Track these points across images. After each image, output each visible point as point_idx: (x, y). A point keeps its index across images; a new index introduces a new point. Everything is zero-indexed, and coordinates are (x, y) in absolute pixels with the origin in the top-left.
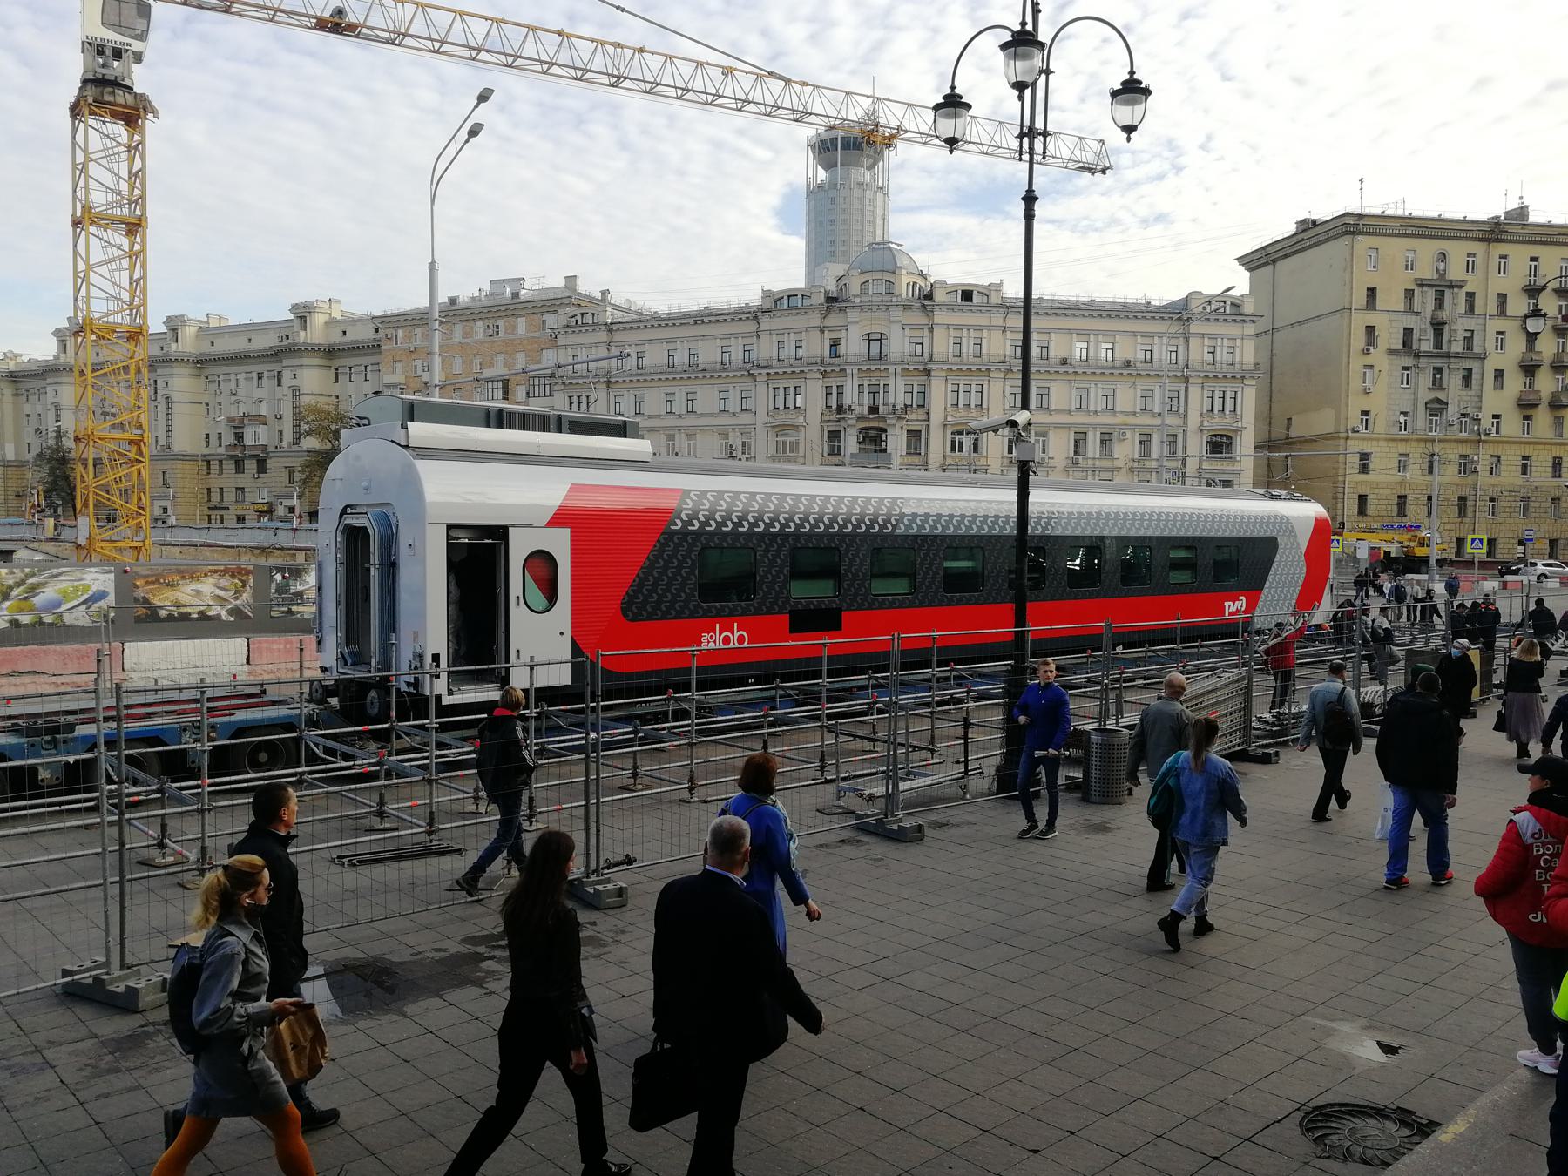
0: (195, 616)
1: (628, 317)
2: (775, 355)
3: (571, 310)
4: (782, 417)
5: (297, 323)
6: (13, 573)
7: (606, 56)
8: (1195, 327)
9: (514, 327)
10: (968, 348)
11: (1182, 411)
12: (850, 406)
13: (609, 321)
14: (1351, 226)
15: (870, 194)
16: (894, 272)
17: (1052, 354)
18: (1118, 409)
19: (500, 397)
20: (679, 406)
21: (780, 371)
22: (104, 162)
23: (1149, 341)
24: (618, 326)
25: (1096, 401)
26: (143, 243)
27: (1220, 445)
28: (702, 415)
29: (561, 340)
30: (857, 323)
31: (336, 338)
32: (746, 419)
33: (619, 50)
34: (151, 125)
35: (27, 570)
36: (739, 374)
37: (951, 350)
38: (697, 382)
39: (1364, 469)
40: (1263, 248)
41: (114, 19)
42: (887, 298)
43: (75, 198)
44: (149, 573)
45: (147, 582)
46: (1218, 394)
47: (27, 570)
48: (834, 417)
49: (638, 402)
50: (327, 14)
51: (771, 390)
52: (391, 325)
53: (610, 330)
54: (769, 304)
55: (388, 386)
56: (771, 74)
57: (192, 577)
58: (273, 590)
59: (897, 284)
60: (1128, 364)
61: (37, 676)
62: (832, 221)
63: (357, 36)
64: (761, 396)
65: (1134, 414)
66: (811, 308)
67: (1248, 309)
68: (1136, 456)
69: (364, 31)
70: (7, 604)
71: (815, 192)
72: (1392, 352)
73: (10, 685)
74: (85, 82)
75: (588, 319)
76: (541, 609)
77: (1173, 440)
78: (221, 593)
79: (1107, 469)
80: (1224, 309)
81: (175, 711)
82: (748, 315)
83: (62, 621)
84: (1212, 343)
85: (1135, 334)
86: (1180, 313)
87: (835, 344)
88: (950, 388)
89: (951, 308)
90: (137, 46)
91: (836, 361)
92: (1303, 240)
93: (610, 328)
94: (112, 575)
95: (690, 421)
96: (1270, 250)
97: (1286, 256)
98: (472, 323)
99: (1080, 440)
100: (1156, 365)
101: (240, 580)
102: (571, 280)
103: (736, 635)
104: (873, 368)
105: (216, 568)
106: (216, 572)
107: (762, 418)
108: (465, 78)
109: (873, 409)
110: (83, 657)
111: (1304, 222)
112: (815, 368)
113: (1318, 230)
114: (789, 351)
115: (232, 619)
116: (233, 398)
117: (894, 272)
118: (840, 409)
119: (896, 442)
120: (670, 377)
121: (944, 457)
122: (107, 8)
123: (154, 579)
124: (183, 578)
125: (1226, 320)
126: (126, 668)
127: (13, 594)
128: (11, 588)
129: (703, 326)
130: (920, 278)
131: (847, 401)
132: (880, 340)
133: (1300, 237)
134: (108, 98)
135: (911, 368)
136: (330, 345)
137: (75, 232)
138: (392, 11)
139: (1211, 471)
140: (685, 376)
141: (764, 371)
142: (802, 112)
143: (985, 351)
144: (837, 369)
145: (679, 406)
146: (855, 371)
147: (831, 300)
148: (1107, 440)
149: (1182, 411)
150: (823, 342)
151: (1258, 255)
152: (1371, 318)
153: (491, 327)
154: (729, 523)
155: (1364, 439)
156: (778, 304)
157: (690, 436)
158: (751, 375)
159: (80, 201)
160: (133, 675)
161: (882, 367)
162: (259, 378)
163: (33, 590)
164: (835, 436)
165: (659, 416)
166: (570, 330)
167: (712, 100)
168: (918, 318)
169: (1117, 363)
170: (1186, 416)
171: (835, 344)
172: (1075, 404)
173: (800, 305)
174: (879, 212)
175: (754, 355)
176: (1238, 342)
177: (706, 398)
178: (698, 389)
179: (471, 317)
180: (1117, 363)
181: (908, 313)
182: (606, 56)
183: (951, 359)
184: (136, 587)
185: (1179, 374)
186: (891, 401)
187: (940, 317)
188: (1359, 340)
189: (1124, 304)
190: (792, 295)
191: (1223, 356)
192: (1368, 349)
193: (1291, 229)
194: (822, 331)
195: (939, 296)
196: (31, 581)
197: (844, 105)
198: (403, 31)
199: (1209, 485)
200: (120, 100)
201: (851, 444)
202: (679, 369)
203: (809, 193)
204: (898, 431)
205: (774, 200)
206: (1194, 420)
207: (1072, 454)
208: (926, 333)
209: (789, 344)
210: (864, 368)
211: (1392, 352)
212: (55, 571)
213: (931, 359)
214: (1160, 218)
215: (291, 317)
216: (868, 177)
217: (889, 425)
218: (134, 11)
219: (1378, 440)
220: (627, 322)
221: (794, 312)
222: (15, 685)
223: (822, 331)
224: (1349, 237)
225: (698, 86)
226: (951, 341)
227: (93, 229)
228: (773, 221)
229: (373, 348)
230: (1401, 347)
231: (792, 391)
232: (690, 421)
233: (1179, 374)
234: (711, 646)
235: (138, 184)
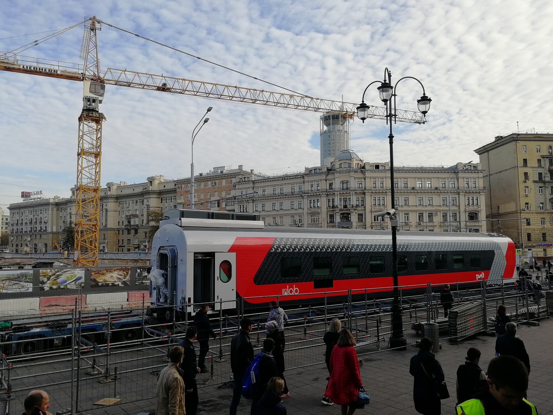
1: (260, 178)
2: (310, 189)
3: (240, 177)
4: (313, 210)
5: (149, 184)
6: (51, 271)
7: (251, 93)
8: (460, 175)
9: (221, 183)
10: (378, 185)
11: (458, 205)
12: (337, 206)
13: (253, 180)
14: (515, 138)
15: (342, 134)
16: (351, 160)
17: (409, 186)
18: (434, 205)
19: (217, 206)
20: (277, 207)
21: (312, 194)
22: (88, 135)
23: (444, 180)
24: (256, 181)
25: (426, 202)
26: (100, 160)
27: (473, 216)
28: (285, 210)
29: (237, 187)
30: (338, 177)
31: (162, 188)
32: (300, 211)
33: (255, 91)
34: (104, 123)
35: (56, 270)
36: (298, 196)
37: (372, 186)
38: (283, 199)
39: (528, 224)
40: (483, 147)
41: (93, 90)
42: (349, 169)
43: (79, 146)
44: (96, 270)
45: (95, 273)
46: (471, 198)
47: (56, 270)
48: (331, 210)
49: (263, 206)
50: (161, 85)
51: (309, 201)
52: (180, 183)
53: (254, 183)
54: (308, 172)
55: (179, 204)
56: (306, 96)
57: (110, 271)
58: (137, 275)
59: (352, 164)
60: (436, 188)
61: (57, 306)
62: (329, 144)
63: (170, 92)
64: (305, 203)
65: (440, 206)
66: (322, 173)
67: (480, 168)
68: (442, 221)
69: (172, 90)
70: (49, 281)
71: (323, 134)
72: (534, 182)
74: (83, 110)
75: (246, 179)
76: (226, 281)
77: (455, 215)
78: (120, 277)
79: (431, 226)
80: (470, 168)
81: (101, 319)
82: (301, 176)
84: (467, 180)
85: (438, 178)
86: (454, 170)
87: (331, 185)
88: (372, 199)
89: (371, 171)
90: (100, 98)
91: (331, 190)
92: (498, 143)
93: (254, 182)
95: (281, 212)
96: (486, 147)
97: (492, 149)
98: (207, 182)
99: (421, 216)
100: (447, 188)
102: (241, 166)
103: (295, 289)
104: (345, 192)
105: (118, 268)
106: (118, 269)
107: (306, 210)
108: (206, 103)
109: (345, 206)
111: (498, 137)
112: (324, 193)
113: (503, 140)
114: (315, 188)
115: (123, 286)
116: (128, 209)
117: (351, 160)
118: (333, 207)
119: (354, 218)
120: (274, 198)
121: (372, 223)
122: (91, 87)
123: (97, 272)
124: (107, 272)
125: (472, 172)
126: (87, 303)
127: (51, 278)
128: (51, 276)
129: (285, 180)
130: (361, 162)
131: (336, 204)
132: (347, 183)
133: (497, 142)
134: (90, 115)
135: (358, 192)
136: (160, 191)
137: (78, 157)
138: (181, 84)
139: (470, 226)
140: (279, 197)
141: (307, 195)
142: (317, 108)
143: (384, 185)
144: (332, 193)
145: (277, 207)
146: (338, 194)
147: (329, 170)
148: (430, 216)
149: (458, 205)
150: (326, 184)
151: (482, 149)
152: (526, 170)
153: (214, 183)
154: (291, 249)
155: (527, 213)
156: (310, 172)
157: (281, 217)
158: (301, 196)
159: (80, 148)
160: (89, 306)
161: (348, 192)
162: (137, 202)
163: (58, 277)
164: (332, 217)
165: (270, 211)
166: (240, 183)
167: (286, 106)
168: (361, 175)
169: (432, 188)
170: (459, 206)
171: (331, 185)
172: (418, 203)
173: (318, 172)
174: (345, 139)
175: (303, 189)
176: (477, 180)
177: (287, 204)
178: (283, 201)
179: (207, 180)
180: (432, 188)
181: (357, 173)
182: (251, 93)
183: (373, 189)
184: (92, 275)
185: (456, 192)
186: (352, 203)
187: (368, 174)
188: (522, 178)
189: (434, 168)
190: (315, 169)
191: (471, 185)
192: (526, 181)
193: (493, 140)
194: (326, 181)
195: (367, 167)
196: (57, 274)
197: (332, 105)
198: (185, 89)
199: (470, 231)
200: (94, 115)
201: (338, 219)
202: (277, 195)
203: (321, 134)
204: (354, 214)
205: (309, 137)
206: (462, 208)
207: (418, 221)
208: (363, 180)
209: (315, 186)
210: (342, 193)
211: (534, 182)
212: (65, 270)
213: (365, 189)
214: (445, 138)
215: (147, 182)
216: (341, 128)
217: (351, 212)
218: (100, 88)
219: (533, 213)
220: (259, 180)
221: (316, 175)
222: (50, 310)
223: (326, 181)
224: (514, 143)
225: (282, 101)
226: (372, 182)
227: (84, 156)
228: (309, 144)
229: (174, 191)
230: (538, 180)
231: (316, 201)
232: (281, 212)
233: (456, 192)
234: (286, 294)
235: (99, 142)
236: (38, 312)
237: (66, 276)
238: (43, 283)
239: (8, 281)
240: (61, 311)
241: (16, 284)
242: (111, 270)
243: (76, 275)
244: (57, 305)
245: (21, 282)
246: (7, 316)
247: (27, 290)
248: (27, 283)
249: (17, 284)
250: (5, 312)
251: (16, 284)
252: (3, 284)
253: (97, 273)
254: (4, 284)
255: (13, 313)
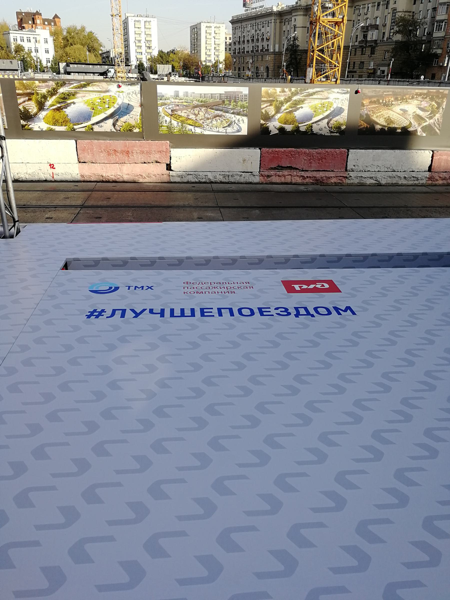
0: (399, 131)
44: (373, 94)
45: (371, 102)
57: (402, 99)
73: (276, 175)
78: (421, 113)
83: (312, 130)
94: (348, 96)
101: (436, 102)
106: (420, 94)
110: (322, 158)
115: (424, 135)
123: (375, 99)
124: (396, 99)
126: (348, 169)
127: (283, 108)
128: (282, 103)
160: (351, 174)
163: (296, 105)
184: (363, 105)
196: (295, 98)
212: (311, 91)
222: (279, 176)
236: (257, 179)
237: (310, 104)
238: (268, 118)
239: (203, 109)
240: (299, 180)
241: (218, 116)
242: (405, 95)
243: (332, 104)
244: (290, 168)
245: (227, 112)
246: (204, 180)
247: (238, 131)
248: (238, 117)
249: (220, 116)
250: (201, 174)
251: (218, 116)
252: (195, 114)
253: (374, 102)
254: (196, 115)
255: (215, 177)
